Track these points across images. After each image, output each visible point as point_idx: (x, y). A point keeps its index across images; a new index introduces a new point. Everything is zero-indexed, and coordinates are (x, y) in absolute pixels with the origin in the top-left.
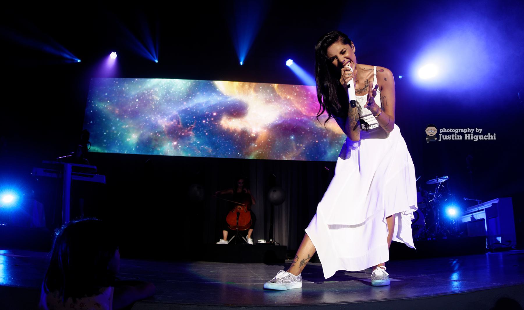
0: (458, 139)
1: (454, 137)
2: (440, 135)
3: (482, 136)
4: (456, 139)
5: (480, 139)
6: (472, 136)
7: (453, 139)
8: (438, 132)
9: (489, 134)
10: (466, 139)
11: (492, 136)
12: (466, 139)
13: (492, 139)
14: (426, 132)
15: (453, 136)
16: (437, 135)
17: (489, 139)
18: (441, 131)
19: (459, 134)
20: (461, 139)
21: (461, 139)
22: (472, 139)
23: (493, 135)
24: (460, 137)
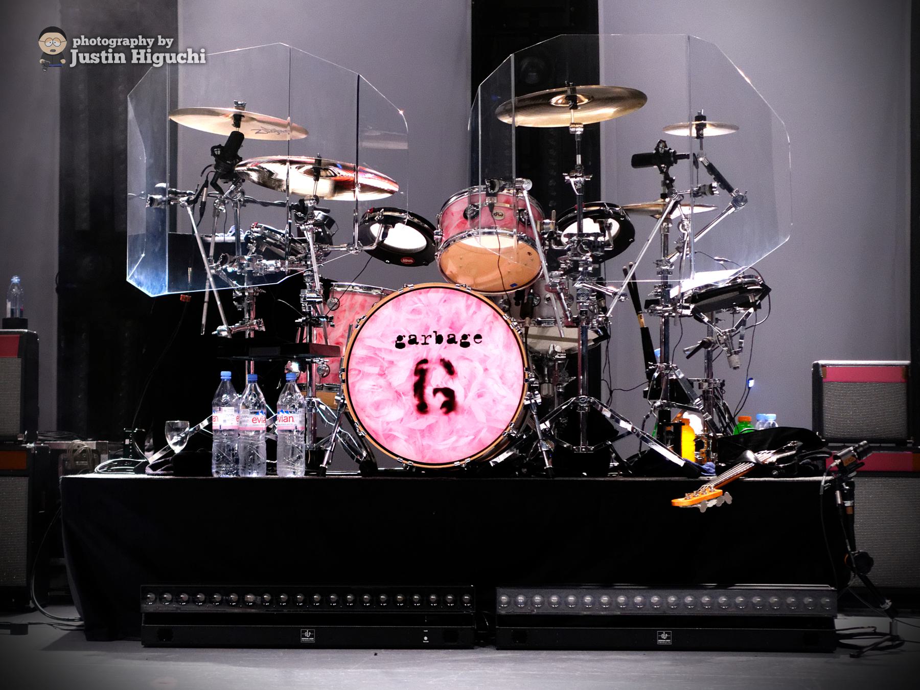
0: (117, 61)
1: (107, 58)
4: (110, 61)
5: (168, 61)
7: (104, 61)
10: (134, 61)
12: (134, 61)
13: (197, 61)
17: (190, 61)
21: (123, 61)
22: (149, 61)
24: (120, 59)
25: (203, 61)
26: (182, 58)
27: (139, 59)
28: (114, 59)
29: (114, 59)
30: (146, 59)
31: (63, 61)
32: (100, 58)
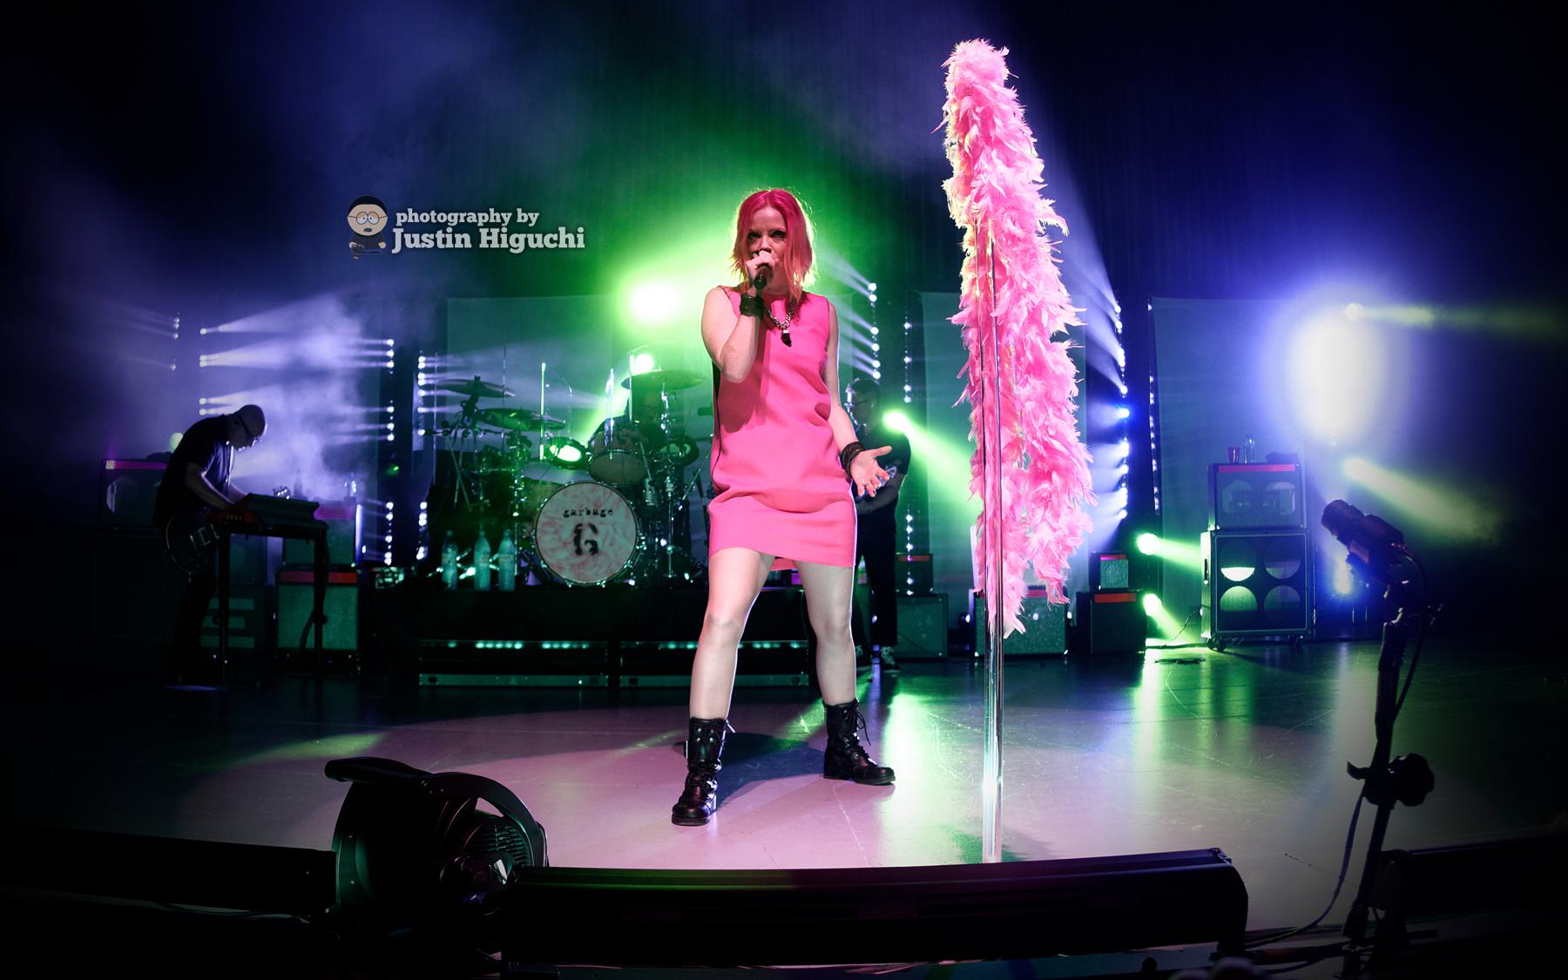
1: (444, 241)
2: (398, 232)
3: (539, 236)
5: (532, 245)
6: (504, 237)
8: (392, 223)
9: (562, 230)
11: (571, 237)
14: (351, 221)
15: (440, 235)
16: (387, 234)
17: (563, 245)
18: (401, 218)
19: (459, 228)
20: (468, 245)
23: (575, 233)
25: (581, 245)
26: (552, 241)
27: (489, 242)
28: (454, 241)
29: (454, 241)
30: (500, 241)
31: (382, 245)
32: (435, 240)
